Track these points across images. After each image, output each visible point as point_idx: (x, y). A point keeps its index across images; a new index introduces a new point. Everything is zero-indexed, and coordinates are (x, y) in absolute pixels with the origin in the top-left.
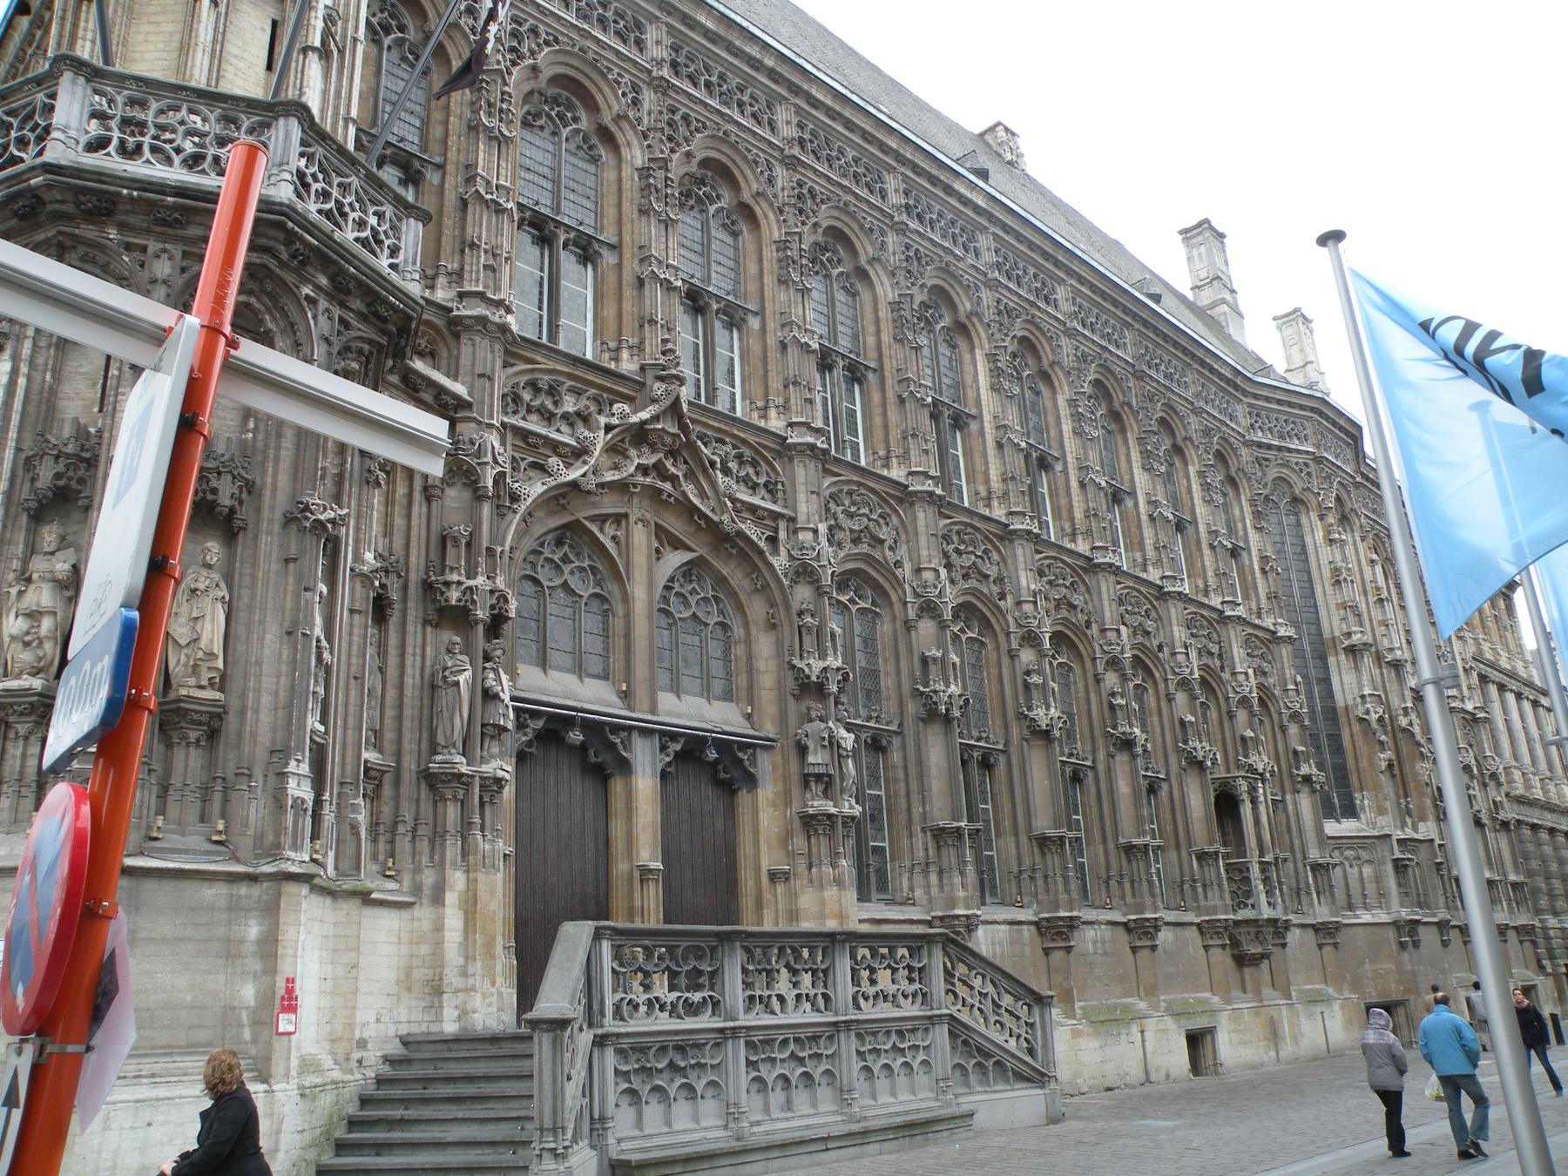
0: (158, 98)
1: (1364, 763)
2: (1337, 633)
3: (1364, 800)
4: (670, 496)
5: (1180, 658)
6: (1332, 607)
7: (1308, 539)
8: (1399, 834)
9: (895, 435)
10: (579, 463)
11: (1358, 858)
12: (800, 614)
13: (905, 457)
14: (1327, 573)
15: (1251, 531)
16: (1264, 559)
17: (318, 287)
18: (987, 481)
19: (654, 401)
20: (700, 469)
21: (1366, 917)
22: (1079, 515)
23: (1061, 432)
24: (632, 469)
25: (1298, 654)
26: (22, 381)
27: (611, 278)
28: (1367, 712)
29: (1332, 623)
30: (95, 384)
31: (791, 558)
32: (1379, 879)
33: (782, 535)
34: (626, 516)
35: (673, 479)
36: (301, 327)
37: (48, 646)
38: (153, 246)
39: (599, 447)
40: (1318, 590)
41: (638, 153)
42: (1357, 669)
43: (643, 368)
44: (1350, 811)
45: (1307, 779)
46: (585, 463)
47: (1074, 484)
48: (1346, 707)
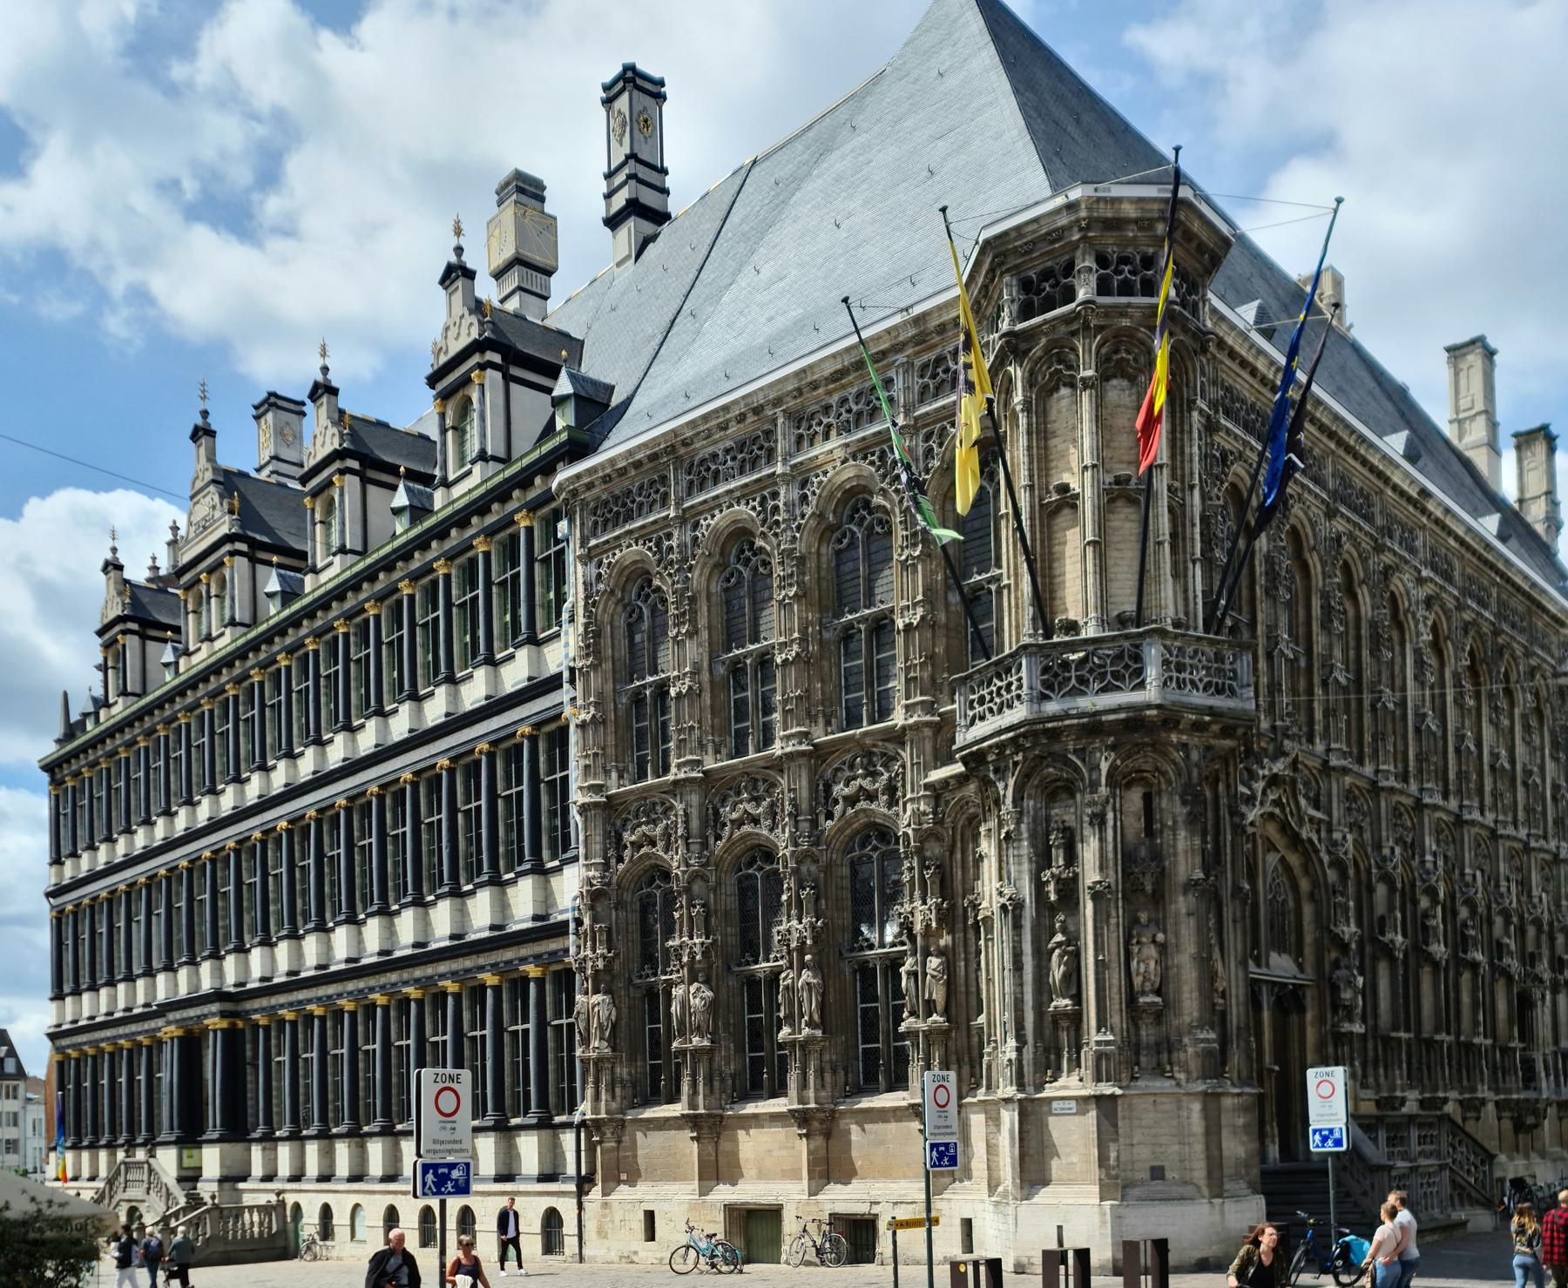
9: (1368, 738)
12: (1334, 892)
13: (1375, 756)
19: (1286, 754)
22: (1452, 776)
31: (1329, 853)
33: (1323, 834)
43: (1274, 728)
47: (1451, 749)
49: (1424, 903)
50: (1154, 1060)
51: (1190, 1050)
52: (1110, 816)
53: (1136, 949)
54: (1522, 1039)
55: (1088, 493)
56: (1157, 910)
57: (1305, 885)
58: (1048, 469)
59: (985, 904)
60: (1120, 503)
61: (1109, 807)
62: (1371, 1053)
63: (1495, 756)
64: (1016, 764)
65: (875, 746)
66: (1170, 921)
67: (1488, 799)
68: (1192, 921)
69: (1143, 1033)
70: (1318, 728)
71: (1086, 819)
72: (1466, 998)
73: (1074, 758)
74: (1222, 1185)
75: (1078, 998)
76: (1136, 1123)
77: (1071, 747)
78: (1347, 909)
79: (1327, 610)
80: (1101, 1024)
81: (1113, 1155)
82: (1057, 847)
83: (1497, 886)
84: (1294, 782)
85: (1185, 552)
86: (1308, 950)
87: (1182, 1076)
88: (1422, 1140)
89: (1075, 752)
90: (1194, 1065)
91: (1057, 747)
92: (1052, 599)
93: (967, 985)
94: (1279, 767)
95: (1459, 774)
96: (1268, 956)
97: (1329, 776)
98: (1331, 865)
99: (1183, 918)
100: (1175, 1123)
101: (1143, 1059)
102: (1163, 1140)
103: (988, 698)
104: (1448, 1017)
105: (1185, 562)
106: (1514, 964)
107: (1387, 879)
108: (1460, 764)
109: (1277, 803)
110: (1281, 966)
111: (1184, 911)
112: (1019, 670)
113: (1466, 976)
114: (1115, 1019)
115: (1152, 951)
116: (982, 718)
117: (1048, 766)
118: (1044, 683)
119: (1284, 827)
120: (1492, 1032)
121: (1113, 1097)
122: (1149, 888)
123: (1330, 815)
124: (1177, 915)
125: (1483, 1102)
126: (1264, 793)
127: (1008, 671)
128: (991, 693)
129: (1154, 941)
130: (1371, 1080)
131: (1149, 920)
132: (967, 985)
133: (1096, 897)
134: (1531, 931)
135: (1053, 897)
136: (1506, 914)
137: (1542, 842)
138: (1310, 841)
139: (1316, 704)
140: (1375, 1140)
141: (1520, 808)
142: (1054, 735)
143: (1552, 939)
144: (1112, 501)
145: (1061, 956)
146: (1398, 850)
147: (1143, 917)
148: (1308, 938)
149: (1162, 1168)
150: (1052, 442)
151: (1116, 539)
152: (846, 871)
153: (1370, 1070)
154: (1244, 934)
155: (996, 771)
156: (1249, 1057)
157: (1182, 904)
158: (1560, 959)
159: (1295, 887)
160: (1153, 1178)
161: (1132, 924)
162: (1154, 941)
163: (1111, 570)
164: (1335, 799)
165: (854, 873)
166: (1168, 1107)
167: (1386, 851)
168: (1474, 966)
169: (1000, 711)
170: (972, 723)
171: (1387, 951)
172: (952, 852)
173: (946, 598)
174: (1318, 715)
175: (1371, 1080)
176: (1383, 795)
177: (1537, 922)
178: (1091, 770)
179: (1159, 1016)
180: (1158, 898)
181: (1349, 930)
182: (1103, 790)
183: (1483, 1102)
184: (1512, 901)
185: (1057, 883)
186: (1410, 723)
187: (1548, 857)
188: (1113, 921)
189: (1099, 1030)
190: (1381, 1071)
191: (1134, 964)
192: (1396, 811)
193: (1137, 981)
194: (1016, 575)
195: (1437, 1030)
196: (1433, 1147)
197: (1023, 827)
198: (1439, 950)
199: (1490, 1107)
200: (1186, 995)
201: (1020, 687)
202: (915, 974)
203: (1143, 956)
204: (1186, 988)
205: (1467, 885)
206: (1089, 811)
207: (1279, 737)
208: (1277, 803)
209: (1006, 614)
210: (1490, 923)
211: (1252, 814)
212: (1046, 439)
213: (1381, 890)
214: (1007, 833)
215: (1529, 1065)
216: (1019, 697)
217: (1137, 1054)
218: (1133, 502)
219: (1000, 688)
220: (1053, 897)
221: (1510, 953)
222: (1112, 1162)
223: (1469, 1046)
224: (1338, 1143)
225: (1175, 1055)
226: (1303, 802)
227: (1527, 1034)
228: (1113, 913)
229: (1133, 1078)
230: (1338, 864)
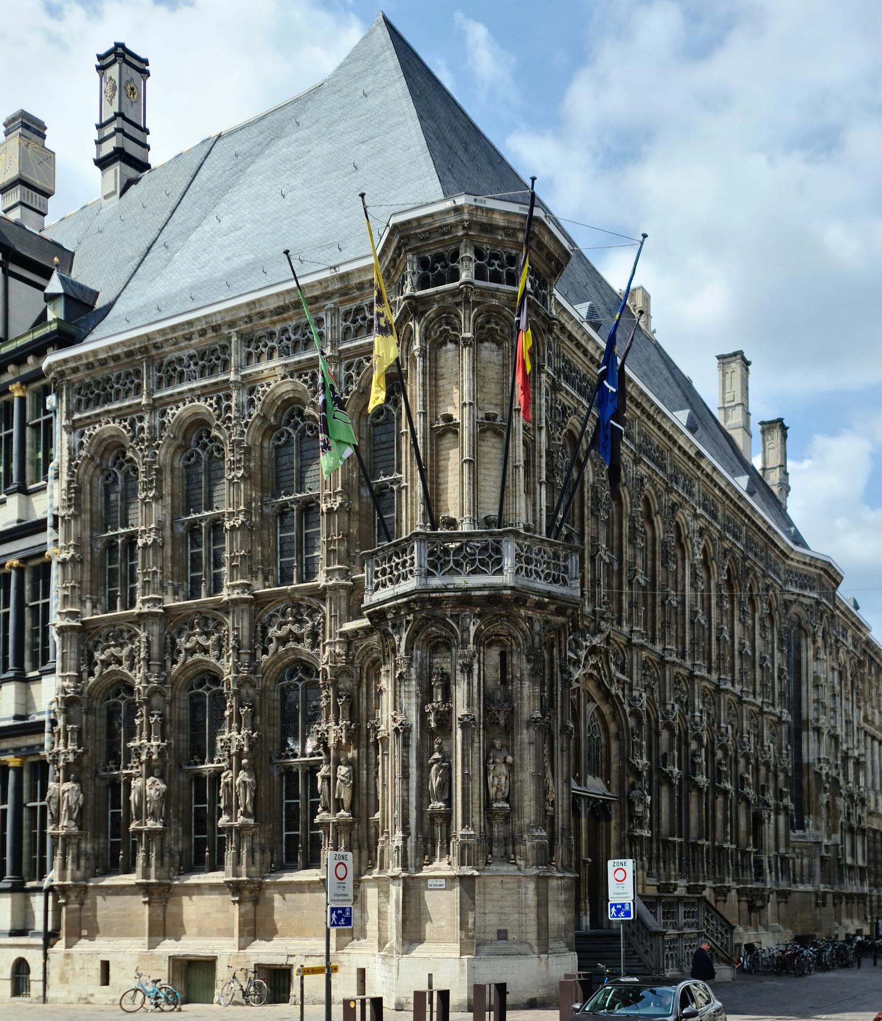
1: (813, 798)
2: (811, 718)
3: (810, 821)
5: (745, 740)
6: (811, 701)
7: (803, 655)
8: (825, 841)
9: (658, 625)
11: (802, 854)
12: (633, 734)
14: (811, 679)
15: (776, 651)
16: (781, 670)
18: (684, 643)
19: (601, 632)
21: (801, 888)
22: (714, 657)
23: (710, 604)
25: (789, 728)
28: (821, 769)
29: (809, 711)
31: (630, 705)
32: (811, 866)
33: (626, 692)
40: (804, 688)
42: (819, 742)
43: (594, 612)
44: (802, 826)
45: (786, 808)
47: (714, 638)
48: (808, 764)
49: (694, 745)
50: (503, 850)
51: (528, 844)
52: (476, 666)
53: (492, 767)
54: (755, 846)
55: (466, 423)
56: (507, 739)
57: (613, 728)
58: (437, 402)
59: (383, 727)
60: (489, 434)
61: (475, 661)
62: (655, 852)
63: (742, 645)
64: (408, 622)
65: (303, 600)
66: (517, 748)
67: (737, 675)
69: (495, 830)
70: (625, 615)
71: (458, 667)
72: (719, 816)
73: (450, 621)
74: (547, 945)
75: (449, 802)
76: (488, 897)
77: (449, 613)
78: (641, 746)
79: (633, 529)
80: (465, 822)
81: (471, 921)
82: (438, 688)
83: (742, 737)
84: (607, 652)
85: (534, 476)
86: (614, 775)
87: (522, 863)
88: (687, 915)
89: (452, 616)
90: (530, 855)
91: (438, 612)
92: (438, 500)
93: (368, 788)
94: (597, 640)
95: (719, 655)
96: (586, 778)
97: (631, 650)
98: (631, 714)
99: (526, 746)
100: (516, 898)
101: (495, 849)
102: (507, 910)
103: (389, 570)
104: (707, 828)
105: (534, 483)
106: (750, 792)
107: (669, 727)
108: (719, 649)
109: (595, 667)
110: (595, 785)
111: (526, 740)
112: (412, 551)
113: (720, 800)
114: (476, 818)
115: (503, 769)
116: (384, 586)
117: (432, 626)
118: (431, 563)
119: (600, 685)
120: (736, 840)
121: (472, 877)
122: (502, 722)
123: (631, 678)
124: (522, 743)
125: (729, 889)
126: (586, 659)
127: (404, 551)
128: (391, 567)
129: (505, 762)
130: (654, 871)
131: (502, 746)
132: (368, 788)
133: (464, 726)
134: (763, 770)
135: (433, 725)
136: (746, 756)
137: (771, 708)
138: (617, 696)
139: (624, 597)
140: (655, 914)
141: (758, 683)
142: (437, 602)
143: (776, 777)
144: (483, 431)
145: (437, 770)
146: (677, 707)
147: (498, 743)
148: (614, 767)
149: (506, 931)
150: (441, 382)
151: (485, 460)
152: (277, 695)
153: (654, 865)
154: (569, 759)
155: (394, 626)
156: (570, 851)
157: (525, 735)
158: (781, 791)
159: (606, 729)
160: (499, 939)
161: (490, 748)
162: (505, 762)
163: (481, 483)
164: (635, 667)
165: (284, 698)
166: (511, 886)
167: (669, 707)
168: (725, 792)
169: (398, 581)
170: (376, 589)
171: (668, 778)
172: (359, 686)
173: (359, 492)
174: (625, 605)
175: (654, 871)
176: (668, 667)
177: (767, 764)
178: (463, 631)
179: (507, 818)
180: (509, 730)
181: (642, 762)
182: (471, 647)
183: (729, 889)
184: (751, 748)
185: (436, 714)
186: (687, 616)
187: (775, 719)
188: (476, 745)
189: (463, 827)
190: (662, 865)
191: (490, 778)
192: (676, 679)
193: (492, 791)
194: (412, 480)
195: (700, 837)
196: (693, 920)
197: (413, 670)
198: (702, 780)
199: (734, 893)
200: (526, 803)
201: (412, 564)
202: (328, 778)
203: (497, 773)
204: (526, 798)
205: (722, 735)
206: (461, 661)
208: (595, 667)
209: (404, 508)
210: (737, 763)
211: (577, 674)
212: (436, 380)
213: (665, 735)
214: (401, 674)
215: (759, 864)
216: (411, 572)
217: (491, 845)
218: (498, 434)
219: (397, 564)
220: (433, 725)
221: (749, 785)
222: (470, 926)
223: (721, 849)
224: (627, 914)
225: (517, 847)
226: (613, 667)
227: (758, 842)
228: (477, 739)
229: (487, 864)
230: (636, 714)
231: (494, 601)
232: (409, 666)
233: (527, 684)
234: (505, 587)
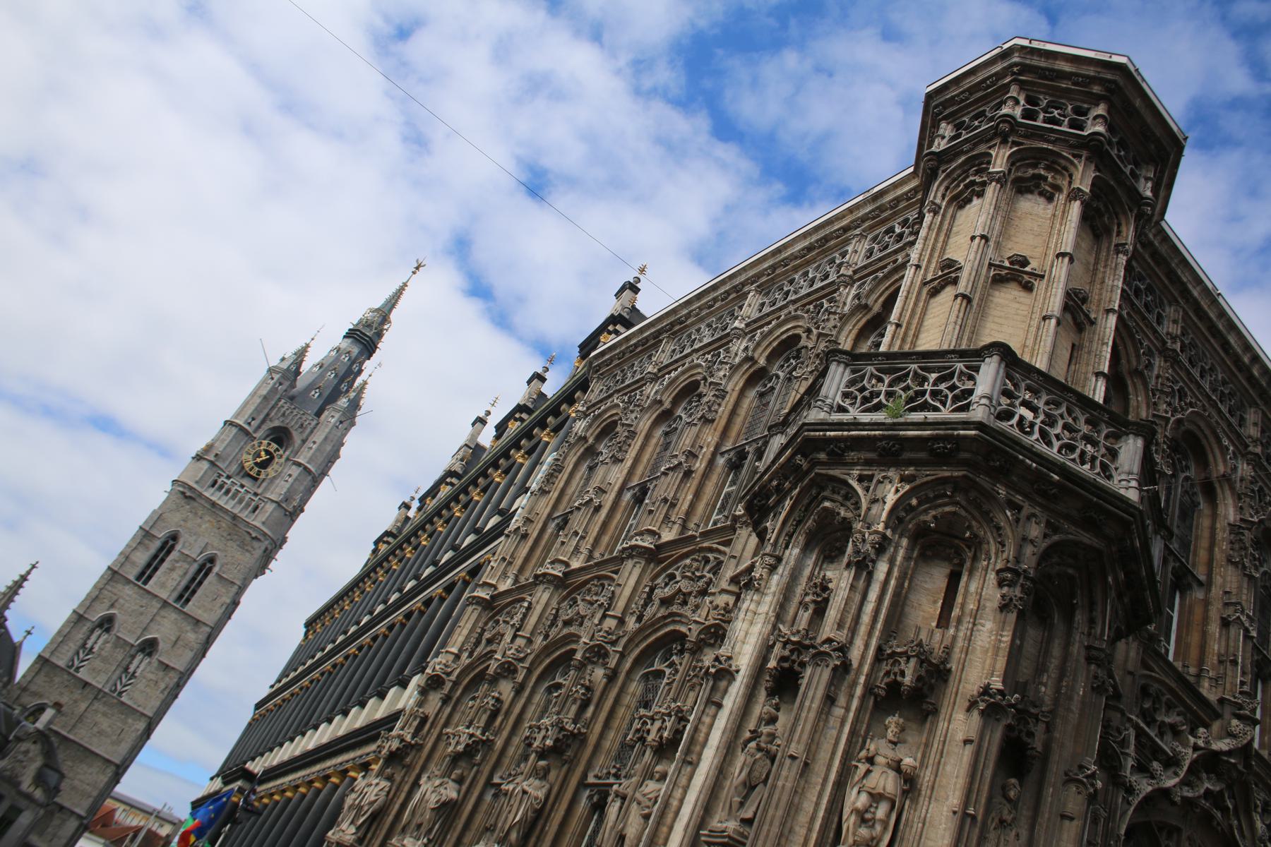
0: (1049, 392)
4: (1218, 824)
10: (1170, 773)
17: (1116, 579)
19: (1231, 735)
20: (1246, 808)
24: (1202, 791)
26: (893, 582)
27: (1198, 611)
30: (935, 602)
34: (1179, 830)
35: (1224, 810)
36: (1099, 608)
37: (878, 828)
38: (1027, 509)
39: (1187, 763)
41: (1231, 511)
46: (1176, 774)
52: (882, 568)
53: (862, 768)
68: (969, 749)
73: (855, 484)
77: (856, 472)
89: (861, 479)
91: (836, 472)
111: (960, 736)
115: (885, 781)
129: (897, 767)
188: (838, 711)
193: (849, 821)
197: (776, 578)
207: (1227, 715)
228: (842, 700)
231: (941, 448)
232: (772, 569)
233: (988, 625)
234: (966, 424)
